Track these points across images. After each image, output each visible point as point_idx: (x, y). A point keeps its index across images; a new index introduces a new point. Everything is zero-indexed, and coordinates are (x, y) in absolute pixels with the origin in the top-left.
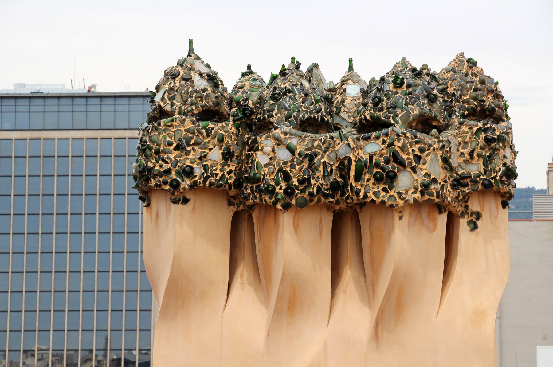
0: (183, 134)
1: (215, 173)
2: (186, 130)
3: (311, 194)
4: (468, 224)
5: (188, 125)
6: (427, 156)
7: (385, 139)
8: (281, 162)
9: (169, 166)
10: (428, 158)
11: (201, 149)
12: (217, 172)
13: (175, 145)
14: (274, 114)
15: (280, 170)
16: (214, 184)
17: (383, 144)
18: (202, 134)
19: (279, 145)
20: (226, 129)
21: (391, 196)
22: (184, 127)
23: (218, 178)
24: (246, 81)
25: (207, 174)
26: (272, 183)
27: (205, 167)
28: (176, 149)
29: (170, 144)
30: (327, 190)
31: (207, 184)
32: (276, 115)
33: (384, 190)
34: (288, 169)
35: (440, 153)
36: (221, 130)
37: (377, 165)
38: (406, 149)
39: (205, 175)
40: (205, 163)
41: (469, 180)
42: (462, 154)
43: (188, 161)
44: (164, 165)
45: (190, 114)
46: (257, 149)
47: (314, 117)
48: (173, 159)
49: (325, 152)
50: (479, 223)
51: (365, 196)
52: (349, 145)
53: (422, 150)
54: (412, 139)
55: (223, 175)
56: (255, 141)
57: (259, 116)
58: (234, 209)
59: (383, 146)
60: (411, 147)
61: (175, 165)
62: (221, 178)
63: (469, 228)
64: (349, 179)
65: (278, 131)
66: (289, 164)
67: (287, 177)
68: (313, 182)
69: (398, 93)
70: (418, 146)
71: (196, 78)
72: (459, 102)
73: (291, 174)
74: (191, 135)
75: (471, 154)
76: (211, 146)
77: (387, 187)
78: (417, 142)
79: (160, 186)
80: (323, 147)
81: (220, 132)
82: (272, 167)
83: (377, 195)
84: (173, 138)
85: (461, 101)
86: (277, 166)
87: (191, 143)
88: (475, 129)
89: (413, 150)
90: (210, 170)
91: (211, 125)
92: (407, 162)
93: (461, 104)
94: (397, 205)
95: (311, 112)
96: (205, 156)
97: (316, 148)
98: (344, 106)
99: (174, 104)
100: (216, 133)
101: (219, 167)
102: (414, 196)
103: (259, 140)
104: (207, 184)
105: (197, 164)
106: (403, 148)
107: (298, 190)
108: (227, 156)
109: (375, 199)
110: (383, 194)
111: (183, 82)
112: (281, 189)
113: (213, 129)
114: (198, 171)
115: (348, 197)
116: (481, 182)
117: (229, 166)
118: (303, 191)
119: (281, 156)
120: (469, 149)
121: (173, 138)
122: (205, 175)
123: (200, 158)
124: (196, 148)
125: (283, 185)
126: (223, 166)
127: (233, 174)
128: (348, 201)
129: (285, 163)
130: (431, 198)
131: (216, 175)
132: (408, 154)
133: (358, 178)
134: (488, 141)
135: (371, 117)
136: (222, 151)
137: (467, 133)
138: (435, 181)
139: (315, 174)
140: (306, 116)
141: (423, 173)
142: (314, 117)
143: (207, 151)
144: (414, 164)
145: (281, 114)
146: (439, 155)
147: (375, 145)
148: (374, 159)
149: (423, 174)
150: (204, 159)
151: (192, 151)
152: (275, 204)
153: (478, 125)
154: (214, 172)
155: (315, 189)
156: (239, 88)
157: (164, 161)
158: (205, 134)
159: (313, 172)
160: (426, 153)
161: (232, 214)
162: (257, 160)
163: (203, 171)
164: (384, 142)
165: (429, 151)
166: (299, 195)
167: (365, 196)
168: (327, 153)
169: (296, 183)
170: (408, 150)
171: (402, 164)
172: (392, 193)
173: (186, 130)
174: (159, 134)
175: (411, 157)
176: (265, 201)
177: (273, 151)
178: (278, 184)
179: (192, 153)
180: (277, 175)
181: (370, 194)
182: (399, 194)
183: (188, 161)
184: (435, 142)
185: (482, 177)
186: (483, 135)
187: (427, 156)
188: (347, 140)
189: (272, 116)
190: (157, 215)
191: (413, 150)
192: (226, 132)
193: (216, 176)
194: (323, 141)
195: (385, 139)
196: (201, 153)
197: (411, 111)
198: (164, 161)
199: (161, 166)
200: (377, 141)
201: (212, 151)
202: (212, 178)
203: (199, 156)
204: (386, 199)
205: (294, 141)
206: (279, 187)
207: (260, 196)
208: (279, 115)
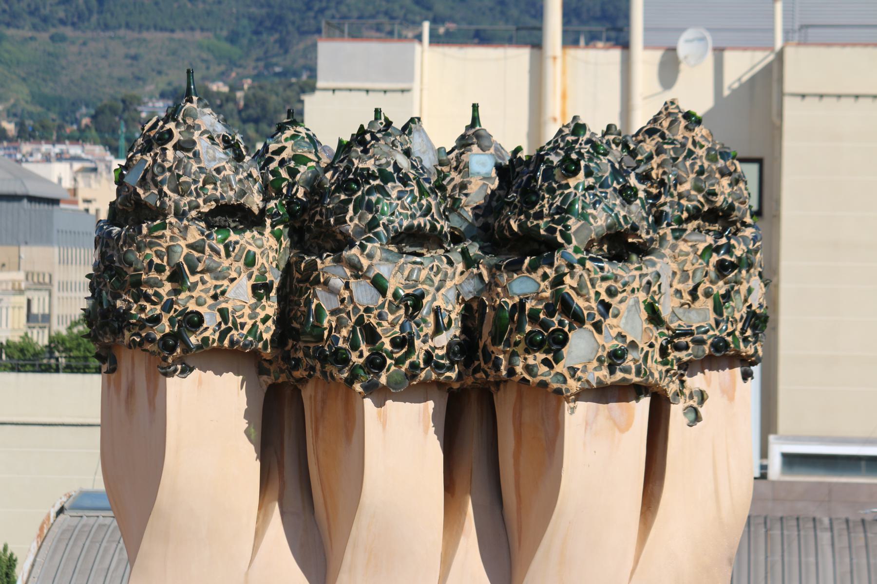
0: (184, 254)
1: (241, 323)
2: (190, 246)
3: (414, 366)
4: (685, 414)
5: (194, 235)
6: (621, 302)
7: (548, 271)
8: (362, 308)
9: (158, 309)
10: (623, 307)
11: (217, 278)
12: (242, 320)
14: (347, 218)
15: (360, 321)
16: (238, 342)
17: (544, 280)
18: (218, 253)
19: (357, 277)
20: (259, 243)
21: (557, 373)
22: (185, 239)
23: (245, 332)
24: (286, 140)
25: (226, 323)
26: (346, 346)
27: (223, 313)
30: (442, 358)
31: (226, 343)
32: (351, 220)
33: (545, 362)
34: (373, 321)
35: (642, 296)
36: (250, 244)
37: (534, 316)
38: (584, 292)
39: (223, 326)
40: (224, 305)
41: (688, 339)
42: (678, 292)
43: (193, 301)
44: (149, 306)
45: (194, 213)
46: (317, 282)
47: (419, 225)
48: (166, 298)
49: (438, 289)
50: (702, 410)
51: (511, 372)
52: (480, 276)
53: (611, 293)
54: (596, 273)
55: (254, 325)
56: (313, 266)
57: (318, 217)
58: (267, 380)
59: (543, 285)
60: (593, 286)
61: (168, 306)
62: (249, 332)
63: (685, 421)
64: (481, 337)
65: (355, 251)
66: (376, 312)
67: (372, 336)
68: (418, 343)
69: (569, 187)
70: (605, 285)
71: (202, 144)
72: (672, 196)
73: (379, 330)
74: (196, 254)
75: (693, 293)
76: (233, 275)
77: (550, 357)
78: (604, 279)
80: (436, 280)
81: (249, 247)
82: (344, 315)
83: (532, 370)
84: (165, 258)
85: (675, 193)
86: (355, 315)
87: (199, 269)
88: (701, 247)
89: (598, 294)
90: (231, 318)
91: (233, 237)
92: (586, 313)
93: (676, 199)
94: (567, 390)
95: (413, 216)
96: (223, 293)
97: (422, 283)
98: (466, 195)
99: (166, 195)
100: (243, 249)
101: (247, 311)
102: (598, 374)
103: (320, 266)
104: (226, 343)
105: (210, 307)
106: (578, 291)
107: (392, 358)
108: (260, 289)
109: (528, 377)
110: (544, 369)
111: (180, 154)
112: (361, 356)
113: (237, 243)
114: (211, 319)
115: (477, 370)
116: (709, 342)
117: (264, 308)
118: (399, 362)
119: (361, 299)
120: (691, 284)
121: (165, 258)
122: (223, 326)
123: (215, 297)
124: (206, 277)
125: (364, 347)
126: (253, 308)
127: (270, 323)
128: (478, 376)
129: (368, 310)
130: (627, 376)
131: (243, 325)
132: (588, 300)
133: (497, 338)
134: (723, 268)
135: (519, 226)
136: (252, 282)
137: (687, 254)
138: (633, 345)
139: (422, 330)
140: (405, 223)
141: (614, 332)
142: (419, 225)
143: (226, 283)
144: (598, 318)
145: (360, 219)
146: (641, 299)
147: (529, 282)
148: (528, 306)
149: (614, 335)
150: (221, 299)
151: (200, 284)
152: (350, 381)
153: (705, 241)
154: (239, 321)
155: (422, 356)
156: (274, 153)
157: (148, 298)
158: (223, 253)
159: (418, 325)
160: (619, 297)
161: (265, 388)
162: (315, 301)
163: (219, 319)
164: (545, 276)
165: (624, 294)
166: (393, 368)
168: (443, 291)
169: (388, 346)
170: (588, 293)
171: (578, 319)
172: (560, 368)
173: (190, 246)
174: (139, 249)
175: (594, 305)
177: (347, 286)
178: (355, 347)
179: (200, 287)
180: (354, 331)
181: (519, 369)
182: (573, 370)
183: (193, 301)
184: (635, 277)
185: (711, 333)
186: (715, 258)
187: (621, 302)
188: (478, 268)
189: (345, 222)
190: (131, 391)
191: (598, 294)
192: (259, 247)
193: (242, 328)
194: (435, 269)
195: (548, 271)
196: (216, 287)
197: (592, 220)
198: (148, 298)
199: (142, 309)
200: (533, 275)
201: (235, 282)
202: (234, 332)
203: (212, 292)
204: (548, 379)
205: (384, 270)
206: (357, 353)
207: (323, 367)
208: (356, 221)
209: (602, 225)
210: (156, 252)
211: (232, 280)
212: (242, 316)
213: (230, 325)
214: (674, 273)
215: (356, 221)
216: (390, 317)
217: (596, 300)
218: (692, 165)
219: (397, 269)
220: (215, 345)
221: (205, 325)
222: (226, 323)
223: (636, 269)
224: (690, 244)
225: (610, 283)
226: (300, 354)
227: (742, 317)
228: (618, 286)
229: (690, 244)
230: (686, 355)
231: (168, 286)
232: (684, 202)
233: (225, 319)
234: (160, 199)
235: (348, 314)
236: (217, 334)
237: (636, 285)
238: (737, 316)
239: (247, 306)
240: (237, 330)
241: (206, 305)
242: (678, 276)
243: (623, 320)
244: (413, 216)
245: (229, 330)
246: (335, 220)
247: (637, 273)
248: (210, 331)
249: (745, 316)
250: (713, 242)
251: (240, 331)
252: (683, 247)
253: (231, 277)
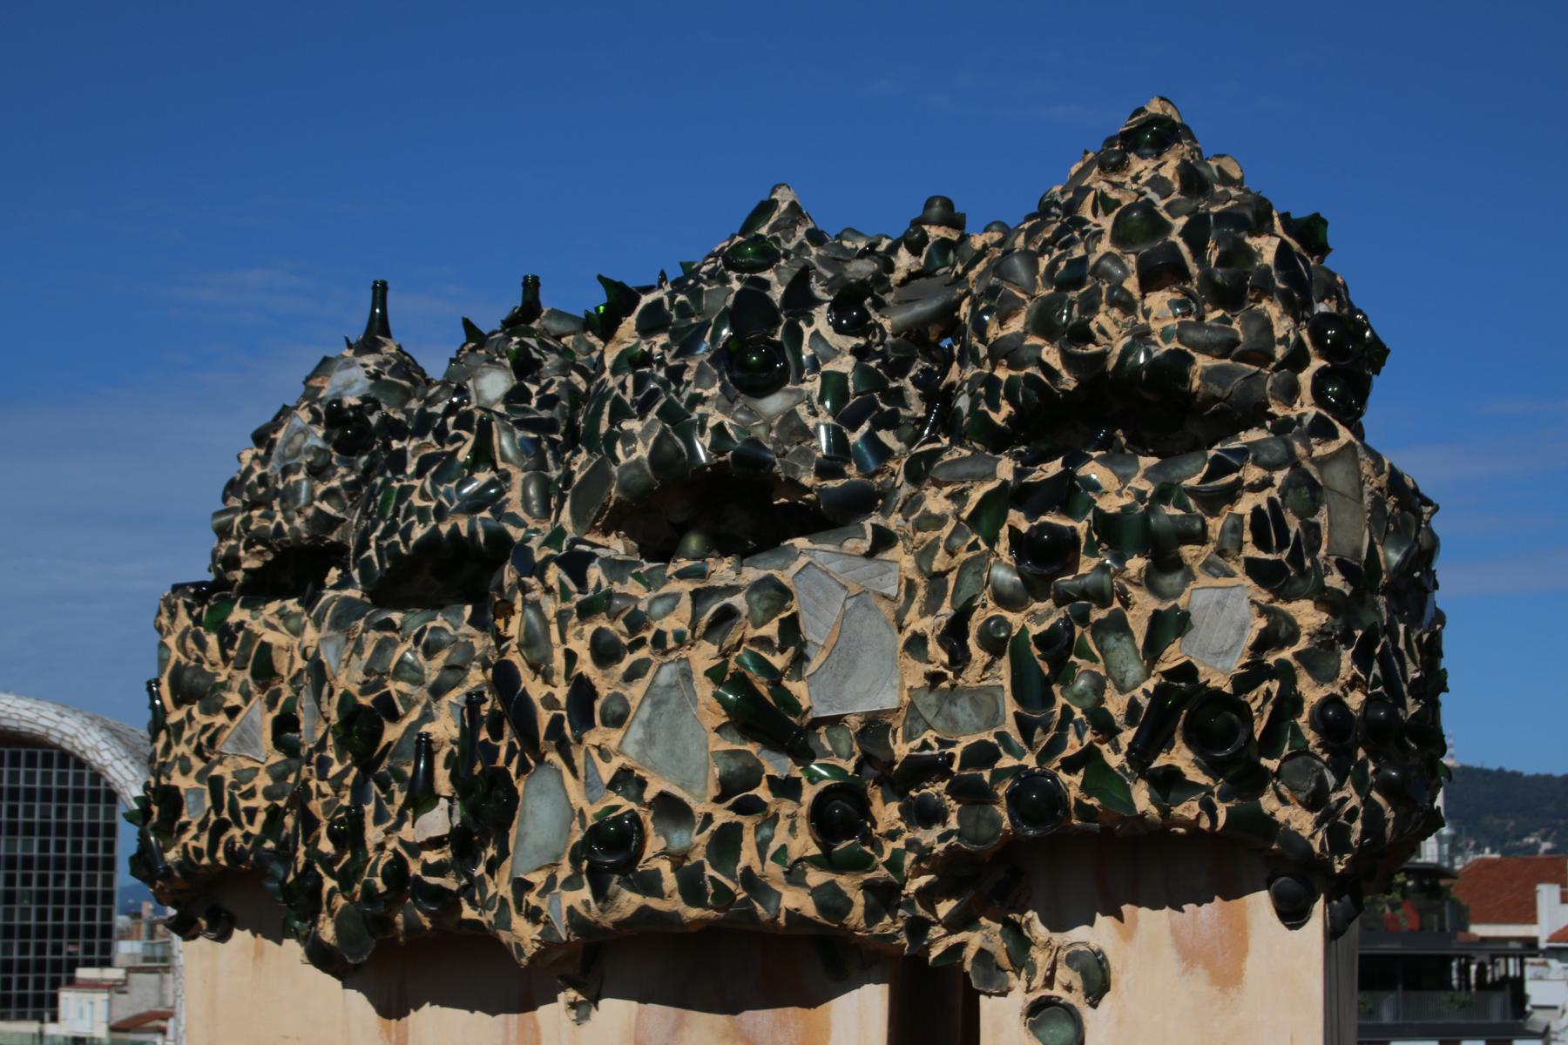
10: (636, 691)
12: (251, 803)
23: (256, 829)
25: (218, 813)
30: (438, 869)
36: (273, 628)
40: (217, 771)
42: (916, 645)
49: (438, 691)
53: (605, 652)
76: (234, 699)
78: (586, 611)
80: (433, 669)
81: (269, 637)
85: (983, 351)
89: (571, 657)
91: (238, 614)
96: (212, 741)
100: (250, 637)
101: (263, 781)
107: (333, 875)
113: (240, 625)
120: (946, 609)
122: (213, 818)
137: (939, 521)
140: (418, 532)
141: (607, 771)
143: (220, 719)
153: (992, 476)
154: (243, 804)
163: (208, 803)
175: (561, 692)
185: (1007, 761)
187: (632, 675)
191: (571, 657)
193: (251, 821)
201: (239, 717)
202: (235, 832)
209: (638, 463)
211: (233, 712)
212: (251, 794)
213: (226, 815)
214: (911, 587)
216: (336, 769)
217: (567, 677)
218: (1053, 266)
219: (351, 645)
220: (205, 861)
221: (184, 819)
222: (218, 813)
223: (682, 575)
224: (947, 490)
225: (602, 622)
227: (1133, 706)
228: (618, 628)
229: (947, 490)
230: (942, 838)
232: (1002, 374)
233: (217, 804)
236: (205, 838)
237: (672, 623)
238: (1115, 705)
239: (263, 767)
240: (240, 826)
241: (193, 774)
242: (921, 593)
243: (636, 732)
244: (440, 513)
245: (222, 826)
247: (687, 587)
248: (193, 830)
249: (1145, 702)
250: (1010, 477)
251: (248, 828)
252: (936, 501)
253: (228, 704)
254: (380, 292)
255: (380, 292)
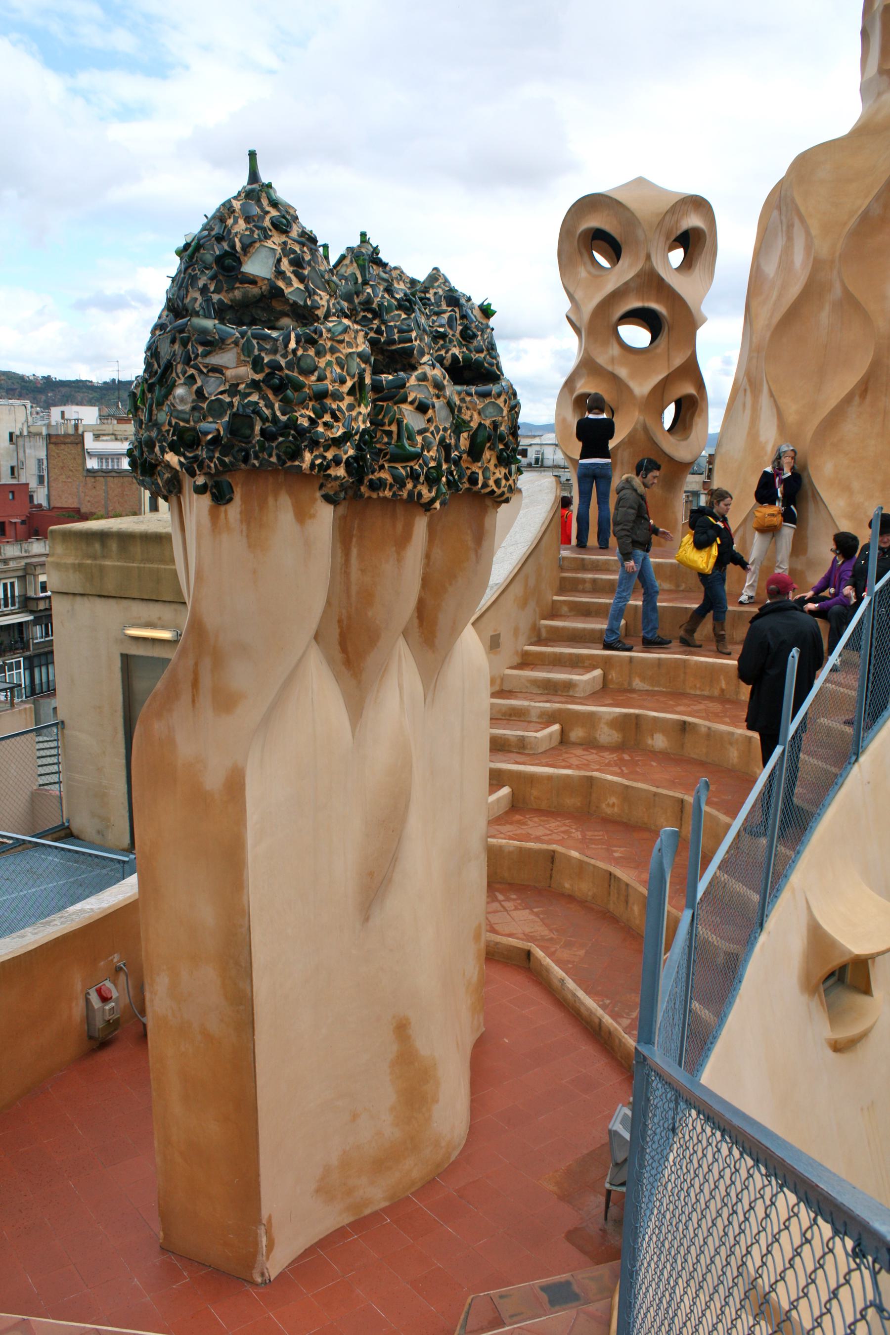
13: (349, 384)
28: (351, 392)
29: (343, 382)
32: (416, 340)
46: (404, 400)
51: (485, 485)
79: (328, 467)
109: (496, 489)
110: (503, 482)
145: (421, 340)
162: (405, 422)
167: (485, 485)
174: (319, 354)
176: (420, 495)
207: (415, 487)
210: (336, 359)
215: (418, 342)
226: (385, 475)
231: (348, 400)
234: (310, 296)
235: (432, 433)
246: (399, 337)
254: (252, 155)
255: (252, 155)
